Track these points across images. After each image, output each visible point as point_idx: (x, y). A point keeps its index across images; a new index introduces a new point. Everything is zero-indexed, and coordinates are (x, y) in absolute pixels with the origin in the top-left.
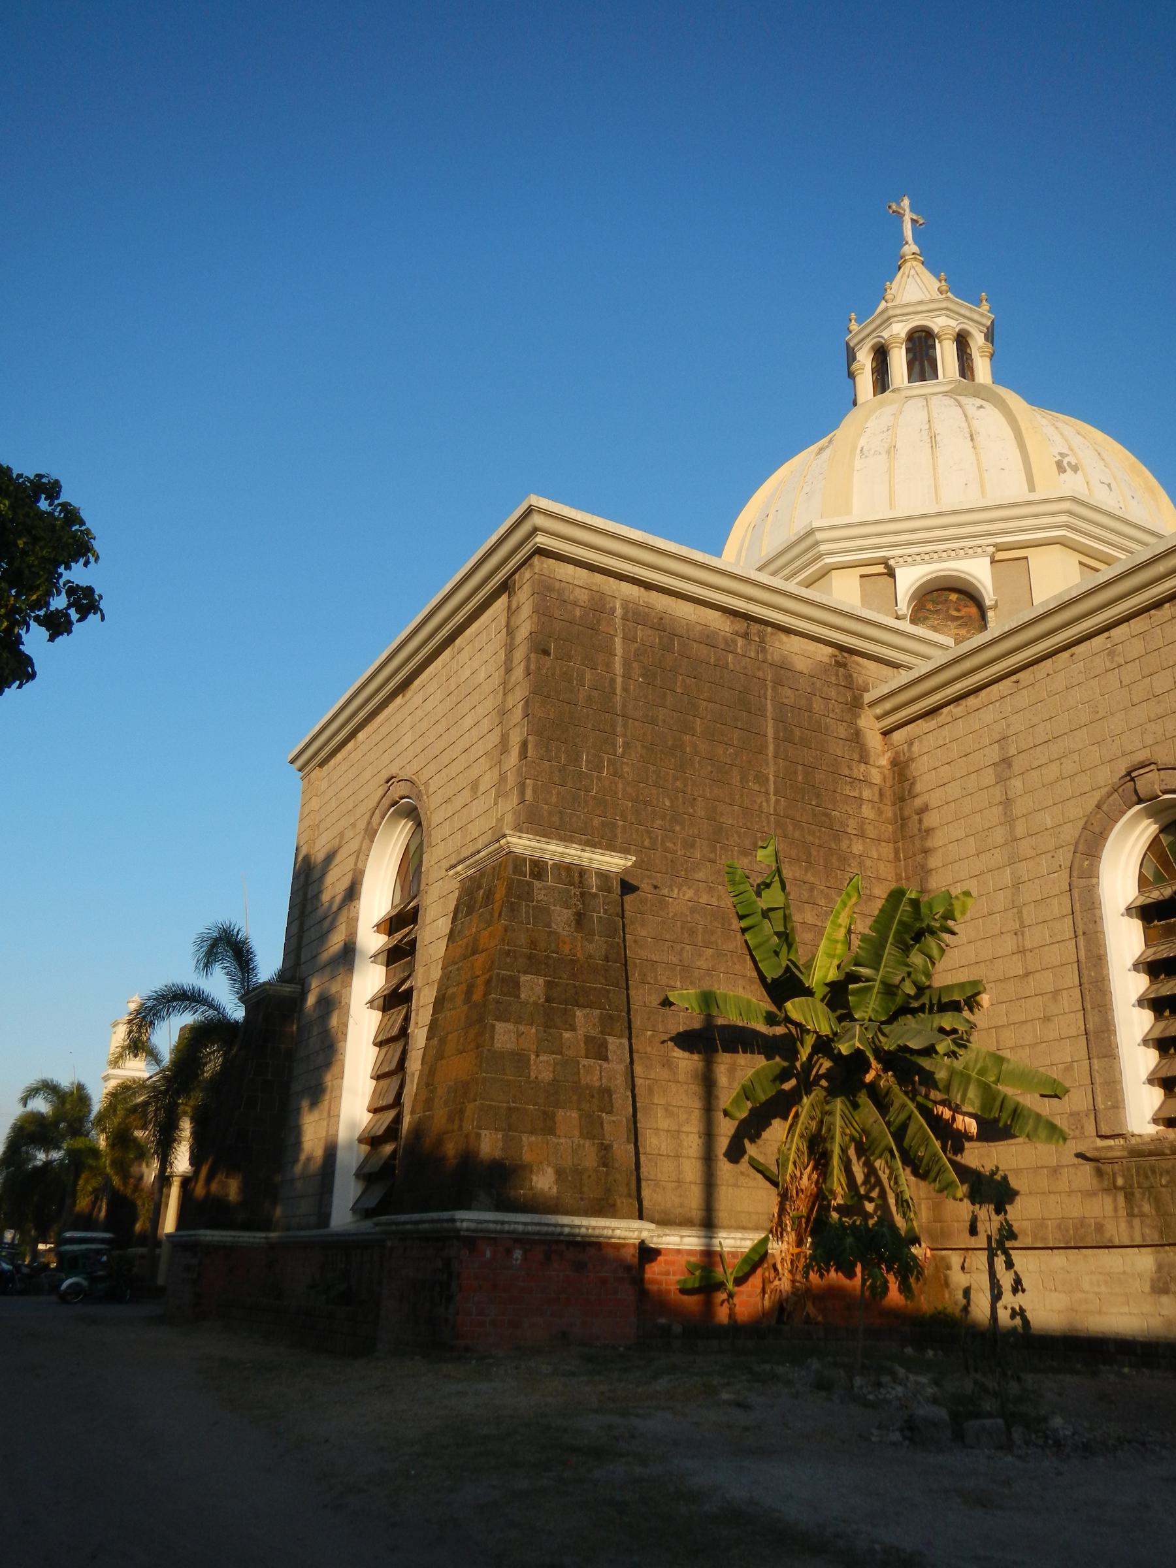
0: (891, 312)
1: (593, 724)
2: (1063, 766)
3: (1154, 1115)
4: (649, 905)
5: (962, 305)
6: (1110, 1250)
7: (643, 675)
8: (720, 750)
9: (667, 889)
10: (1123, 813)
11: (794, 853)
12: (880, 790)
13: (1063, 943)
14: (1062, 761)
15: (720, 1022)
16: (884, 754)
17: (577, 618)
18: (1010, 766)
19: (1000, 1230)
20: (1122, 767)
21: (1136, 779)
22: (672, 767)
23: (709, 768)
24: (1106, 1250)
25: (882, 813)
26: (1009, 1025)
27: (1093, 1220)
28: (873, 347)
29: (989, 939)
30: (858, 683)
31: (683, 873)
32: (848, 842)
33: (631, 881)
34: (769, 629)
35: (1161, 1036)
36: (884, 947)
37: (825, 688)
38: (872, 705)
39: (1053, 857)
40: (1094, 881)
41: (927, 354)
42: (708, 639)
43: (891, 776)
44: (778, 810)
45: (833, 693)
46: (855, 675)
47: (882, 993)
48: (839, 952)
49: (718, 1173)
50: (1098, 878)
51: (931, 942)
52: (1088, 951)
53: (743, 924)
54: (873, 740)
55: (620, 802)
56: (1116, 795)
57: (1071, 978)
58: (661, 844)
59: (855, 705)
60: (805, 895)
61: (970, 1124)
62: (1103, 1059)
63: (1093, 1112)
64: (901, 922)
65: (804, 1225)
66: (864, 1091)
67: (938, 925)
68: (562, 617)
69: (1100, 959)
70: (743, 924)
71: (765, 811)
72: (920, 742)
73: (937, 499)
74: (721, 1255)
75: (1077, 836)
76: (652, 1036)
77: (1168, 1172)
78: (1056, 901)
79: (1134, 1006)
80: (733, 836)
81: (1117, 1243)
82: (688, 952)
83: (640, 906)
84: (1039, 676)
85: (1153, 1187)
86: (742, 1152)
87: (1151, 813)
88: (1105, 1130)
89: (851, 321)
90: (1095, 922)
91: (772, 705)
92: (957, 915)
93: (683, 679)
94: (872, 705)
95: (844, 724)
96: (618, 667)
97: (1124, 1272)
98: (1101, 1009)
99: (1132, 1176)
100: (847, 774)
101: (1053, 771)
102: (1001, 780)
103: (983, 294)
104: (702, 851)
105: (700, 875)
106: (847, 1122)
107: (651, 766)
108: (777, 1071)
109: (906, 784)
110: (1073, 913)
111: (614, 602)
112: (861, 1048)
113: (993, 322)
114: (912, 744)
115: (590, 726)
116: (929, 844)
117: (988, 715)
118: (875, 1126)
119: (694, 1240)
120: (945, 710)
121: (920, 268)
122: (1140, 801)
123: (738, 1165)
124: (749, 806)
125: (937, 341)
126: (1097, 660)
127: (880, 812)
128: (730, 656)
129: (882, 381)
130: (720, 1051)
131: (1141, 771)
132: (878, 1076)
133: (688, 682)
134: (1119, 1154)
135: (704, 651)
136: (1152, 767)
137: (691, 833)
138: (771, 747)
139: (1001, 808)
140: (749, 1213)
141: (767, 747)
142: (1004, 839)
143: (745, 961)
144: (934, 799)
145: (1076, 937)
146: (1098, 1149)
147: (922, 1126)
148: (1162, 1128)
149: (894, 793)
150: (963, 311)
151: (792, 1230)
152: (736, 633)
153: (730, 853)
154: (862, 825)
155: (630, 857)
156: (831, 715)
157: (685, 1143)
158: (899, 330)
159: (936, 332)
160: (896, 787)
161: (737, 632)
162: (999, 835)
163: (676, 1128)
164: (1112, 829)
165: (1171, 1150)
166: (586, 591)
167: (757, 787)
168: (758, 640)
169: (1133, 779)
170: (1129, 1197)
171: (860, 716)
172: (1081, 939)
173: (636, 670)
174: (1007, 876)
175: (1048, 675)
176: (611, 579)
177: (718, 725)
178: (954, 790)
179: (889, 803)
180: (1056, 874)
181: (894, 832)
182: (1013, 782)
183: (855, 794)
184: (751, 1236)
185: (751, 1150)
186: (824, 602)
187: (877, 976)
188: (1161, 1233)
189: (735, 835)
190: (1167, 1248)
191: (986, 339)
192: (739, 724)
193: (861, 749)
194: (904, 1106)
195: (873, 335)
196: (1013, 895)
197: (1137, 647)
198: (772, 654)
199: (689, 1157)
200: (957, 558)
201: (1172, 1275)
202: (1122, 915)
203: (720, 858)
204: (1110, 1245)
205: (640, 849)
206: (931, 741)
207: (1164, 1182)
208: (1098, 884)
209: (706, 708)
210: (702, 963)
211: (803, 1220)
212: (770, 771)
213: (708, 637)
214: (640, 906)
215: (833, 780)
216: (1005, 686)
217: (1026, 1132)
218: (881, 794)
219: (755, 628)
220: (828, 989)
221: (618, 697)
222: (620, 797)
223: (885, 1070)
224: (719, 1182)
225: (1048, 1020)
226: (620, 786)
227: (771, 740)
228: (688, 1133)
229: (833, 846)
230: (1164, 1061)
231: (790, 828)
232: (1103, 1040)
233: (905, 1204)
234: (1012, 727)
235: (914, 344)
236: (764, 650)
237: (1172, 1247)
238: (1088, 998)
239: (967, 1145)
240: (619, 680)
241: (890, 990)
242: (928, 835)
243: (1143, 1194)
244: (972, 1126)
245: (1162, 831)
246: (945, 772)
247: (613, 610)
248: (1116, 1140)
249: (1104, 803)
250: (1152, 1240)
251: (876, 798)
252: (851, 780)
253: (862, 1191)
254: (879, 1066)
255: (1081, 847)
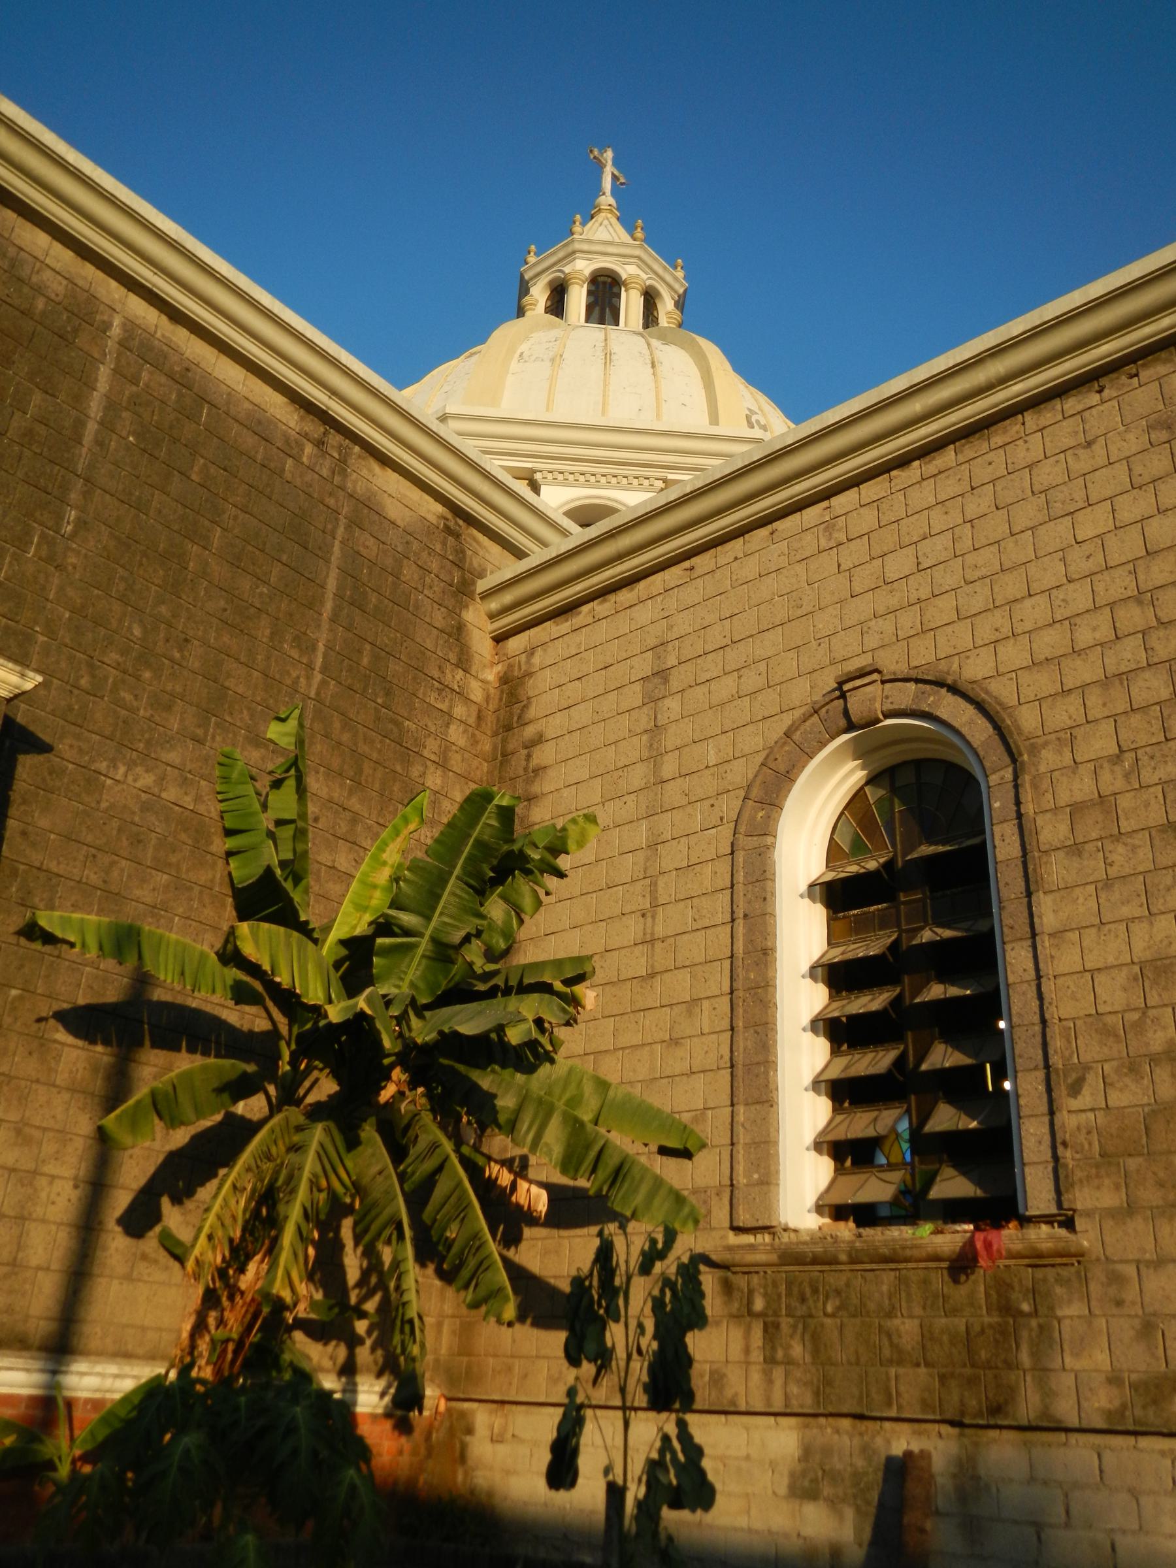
0: (577, 246)
1: (26, 474)
2: (742, 680)
3: (819, 1199)
4: (66, 780)
5: (656, 259)
6: (730, 1417)
7: (137, 435)
8: (246, 584)
9: (105, 764)
10: (824, 745)
11: (336, 763)
12: (479, 711)
13: (712, 930)
14: (741, 673)
15: (158, 995)
16: (492, 666)
17: (37, 311)
18: (666, 681)
19: (654, 1467)
20: (829, 682)
21: (848, 694)
22: (156, 581)
23: (222, 603)
24: (723, 1418)
25: (477, 742)
26: (616, 1050)
27: (707, 1367)
28: (550, 283)
29: (604, 924)
30: (471, 564)
31: (141, 746)
32: (421, 769)
33: (40, 735)
34: (357, 449)
35: (843, 1076)
36: (443, 880)
37: (425, 555)
38: (487, 595)
39: (712, 806)
40: (769, 840)
41: (610, 302)
42: (260, 426)
43: (497, 697)
44: (323, 695)
45: (434, 566)
46: (469, 553)
47: (429, 958)
48: (375, 902)
49: (99, 1253)
50: (775, 837)
51: (522, 886)
52: (750, 941)
53: (231, 843)
54: (481, 644)
55: (49, 605)
56: (815, 718)
57: (718, 980)
58: (111, 691)
59: (463, 590)
60: (343, 828)
61: (538, 1196)
62: (753, 1108)
63: (728, 1190)
64: (479, 843)
65: (230, 1356)
66: (372, 1120)
67: (537, 857)
68: (9, 300)
69: (765, 954)
70: (231, 843)
71: (302, 690)
72: (545, 650)
73: (604, 412)
74: (70, 1404)
75: (751, 776)
76: (20, 998)
77: (838, 1292)
78: (708, 869)
79: (804, 1030)
80: (241, 712)
81: (743, 1408)
82: (122, 870)
83: (48, 778)
84: (722, 561)
85: (811, 1316)
86: (157, 1217)
87: (860, 751)
88: (743, 1219)
89: (529, 253)
90: (765, 899)
91: (342, 549)
92: (571, 845)
93: (205, 465)
94: (487, 595)
95: (443, 609)
96: (95, 406)
97: (748, 1458)
98: (759, 1029)
99: (779, 1296)
100: (436, 676)
101: (725, 688)
102: (652, 700)
103: (679, 261)
104: (182, 720)
105: (173, 757)
106: (328, 1167)
107: (120, 570)
108: (233, 1075)
109: (517, 709)
110: (732, 887)
111: (111, 316)
112: (369, 1012)
113: (685, 291)
114: (532, 654)
115: (20, 474)
116: (536, 788)
117: (643, 614)
118: (380, 1179)
119: (19, 1377)
120: (585, 609)
121: (614, 221)
122: (850, 727)
123: (141, 1242)
124: (277, 677)
125: (623, 289)
126: (808, 537)
127: (475, 742)
128: (290, 462)
129: (557, 304)
130: (147, 1043)
131: (858, 682)
132: (401, 1094)
133: (212, 470)
134: (761, 1257)
135: (249, 441)
136: (875, 676)
137: (169, 688)
138: (329, 605)
139: (645, 737)
140: (144, 1329)
141: (322, 603)
142: (645, 781)
143: (223, 906)
144: (553, 727)
145: (733, 920)
146: (730, 1248)
147: (459, 1184)
148: (827, 1220)
149: (498, 720)
150: (656, 267)
151: (208, 1363)
152: (306, 436)
153: (231, 735)
154: (445, 751)
155: (31, 674)
156: (426, 592)
157: (43, 1195)
158: (584, 267)
159: (624, 276)
160: (502, 712)
161: (307, 434)
162: (638, 776)
163: (31, 1166)
164: (804, 767)
165: (850, 1255)
166: (65, 282)
167: (295, 654)
168: (336, 455)
169: (843, 696)
170: (771, 1330)
171: (467, 607)
172: (740, 922)
173: (128, 423)
174: (640, 835)
175: (736, 559)
176: (114, 284)
177: (250, 548)
178: (582, 715)
179: (489, 733)
180: (714, 830)
181: (490, 772)
182: (668, 702)
183: (444, 706)
184: (136, 1371)
185: (173, 1218)
186: (442, 434)
187: (427, 928)
188: (817, 1394)
189: (245, 712)
190: (822, 1420)
191: (677, 305)
192: (284, 558)
193: (462, 650)
194: (435, 1146)
195: (556, 268)
196: (647, 859)
197: (868, 519)
198: (355, 482)
199: (44, 1221)
200: (618, 487)
201: (827, 1467)
202: (802, 896)
203: (213, 738)
204: (732, 1409)
205: (69, 687)
206: (559, 649)
207: (829, 1309)
208: (773, 845)
209: (236, 518)
210: (145, 894)
211: (231, 1347)
212: (322, 638)
213: (259, 422)
214: (48, 778)
215: (414, 678)
216: (674, 574)
217: (633, 1206)
218: (480, 717)
219: (335, 439)
220: (344, 952)
221: (84, 450)
222: (51, 597)
223: (413, 1085)
224: (96, 1270)
225: (677, 1043)
226: (56, 581)
227: (331, 596)
228: (53, 1177)
229: (399, 768)
230: (839, 1118)
231: (337, 725)
232: (757, 1076)
233: (407, 1328)
234: (675, 629)
235: (597, 287)
236: (343, 473)
237: (831, 1420)
238: (740, 1011)
239: (527, 1232)
240: (91, 427)
241: (444, 953)
242: (535, 776)
243: (795, 1327)
244: (541, 1201)
245: (870, 781)
246: (573, 691)
247: (107, 326)
248: (759, 1236)
249: (797, 729)
250: (802, 1406)
251: (472, 720)
252: (440, 686)
253: (353, 1300)
254: (404, 1077)
255: (755, 793)
